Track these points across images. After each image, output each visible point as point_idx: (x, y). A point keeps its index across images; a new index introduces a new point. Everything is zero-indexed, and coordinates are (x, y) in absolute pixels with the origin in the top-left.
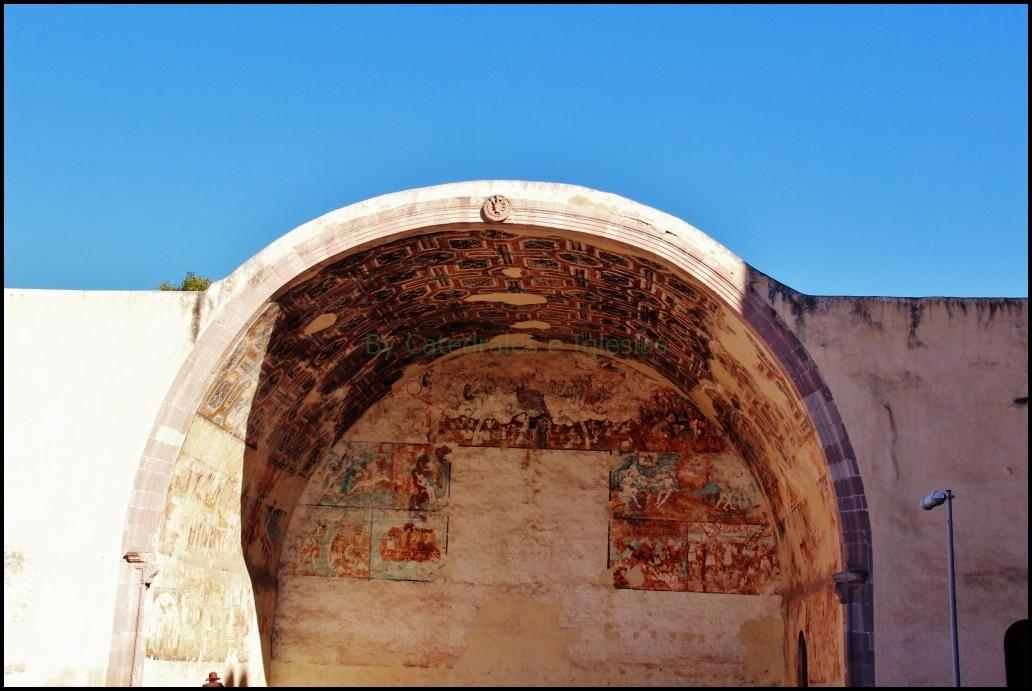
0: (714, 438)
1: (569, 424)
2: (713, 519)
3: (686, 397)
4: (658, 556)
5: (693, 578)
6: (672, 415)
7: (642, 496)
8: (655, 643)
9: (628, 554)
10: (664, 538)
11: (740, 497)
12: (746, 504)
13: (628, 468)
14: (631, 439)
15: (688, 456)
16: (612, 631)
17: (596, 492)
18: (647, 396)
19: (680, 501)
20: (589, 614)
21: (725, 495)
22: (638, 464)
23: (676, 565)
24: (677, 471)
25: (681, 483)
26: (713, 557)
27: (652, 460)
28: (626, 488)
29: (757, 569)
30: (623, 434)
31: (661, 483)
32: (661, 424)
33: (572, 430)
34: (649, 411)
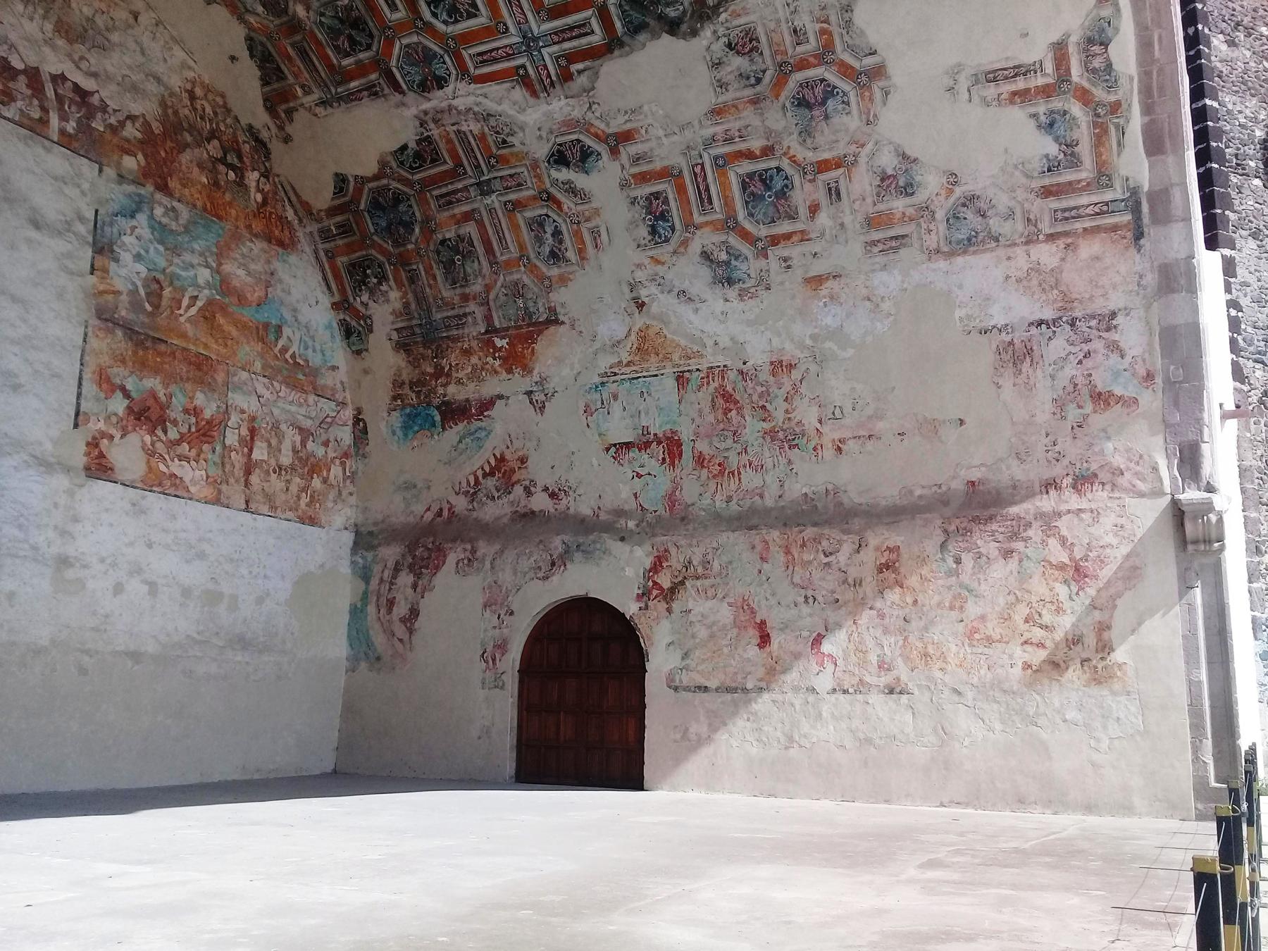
0: (280, 218)
1: (17, 64)
2: (270, 374)
3: (260, 118)
4: (175, 422)
5: (232, 480)
6: (216, 142)
7: (156, 286)
8: (153, 607)
9: (118, 405)
10: (188, 386)
11: (310, 343)
12: (315, 360)
13: (133, 217)
14: (140, 157)
15: (236, 237)
16: (70, 574)
17: (60, 245)
18: (175, 82)
19: (221, 320)
20: (20, 527)
21: (291, 335)
22: (151, 217)
23: (206, 447)
24: (219, 256)
25: (225, 286)
26: (265, 445)
27: (177, 219)
28: (126, 257)
29: (325, 481)
30: (128, 141)
31: (191, 273)
32: (197, 150)
33: (22, 79)
34: (176, 113)
